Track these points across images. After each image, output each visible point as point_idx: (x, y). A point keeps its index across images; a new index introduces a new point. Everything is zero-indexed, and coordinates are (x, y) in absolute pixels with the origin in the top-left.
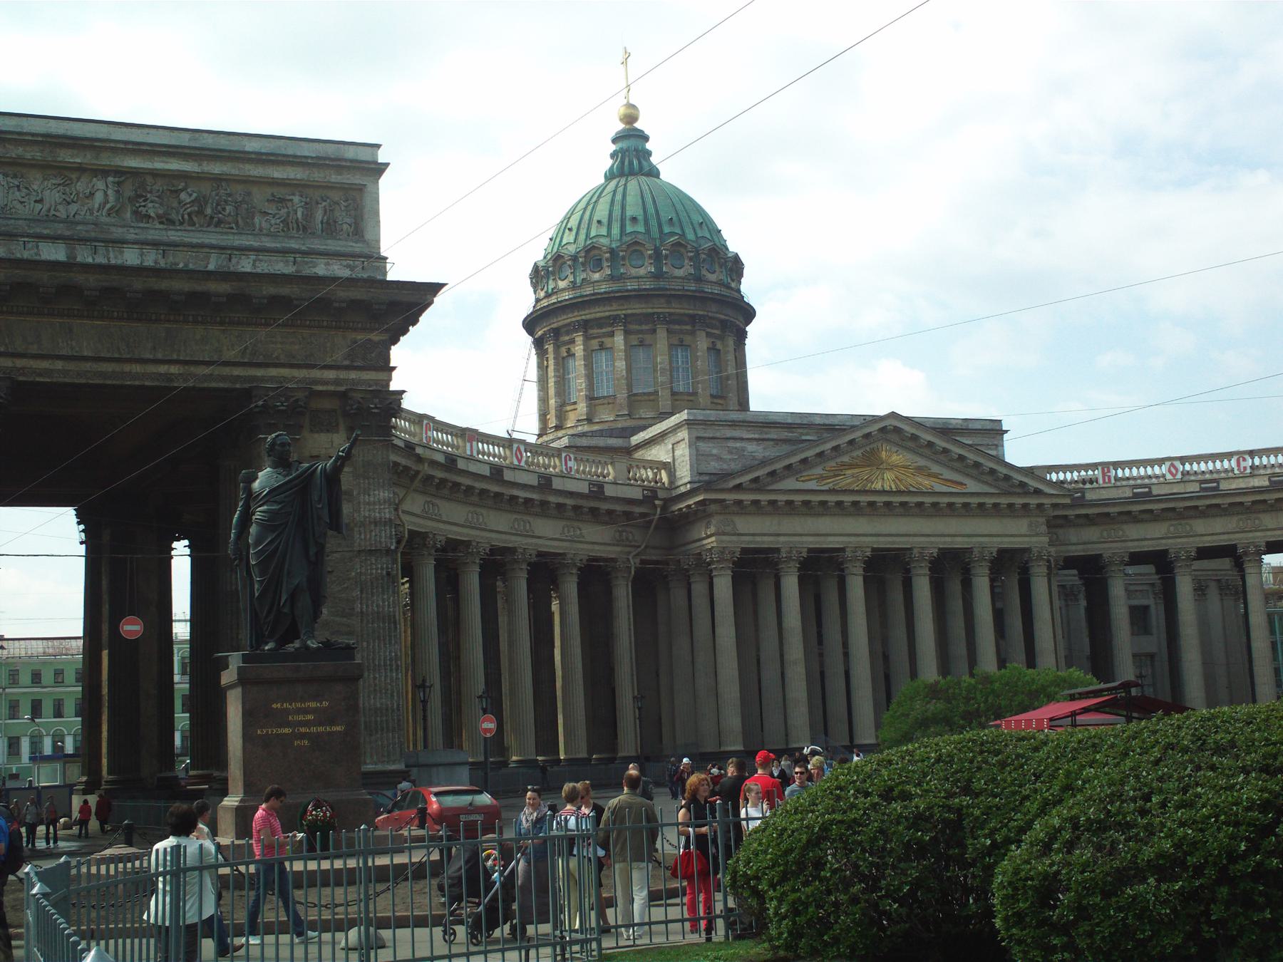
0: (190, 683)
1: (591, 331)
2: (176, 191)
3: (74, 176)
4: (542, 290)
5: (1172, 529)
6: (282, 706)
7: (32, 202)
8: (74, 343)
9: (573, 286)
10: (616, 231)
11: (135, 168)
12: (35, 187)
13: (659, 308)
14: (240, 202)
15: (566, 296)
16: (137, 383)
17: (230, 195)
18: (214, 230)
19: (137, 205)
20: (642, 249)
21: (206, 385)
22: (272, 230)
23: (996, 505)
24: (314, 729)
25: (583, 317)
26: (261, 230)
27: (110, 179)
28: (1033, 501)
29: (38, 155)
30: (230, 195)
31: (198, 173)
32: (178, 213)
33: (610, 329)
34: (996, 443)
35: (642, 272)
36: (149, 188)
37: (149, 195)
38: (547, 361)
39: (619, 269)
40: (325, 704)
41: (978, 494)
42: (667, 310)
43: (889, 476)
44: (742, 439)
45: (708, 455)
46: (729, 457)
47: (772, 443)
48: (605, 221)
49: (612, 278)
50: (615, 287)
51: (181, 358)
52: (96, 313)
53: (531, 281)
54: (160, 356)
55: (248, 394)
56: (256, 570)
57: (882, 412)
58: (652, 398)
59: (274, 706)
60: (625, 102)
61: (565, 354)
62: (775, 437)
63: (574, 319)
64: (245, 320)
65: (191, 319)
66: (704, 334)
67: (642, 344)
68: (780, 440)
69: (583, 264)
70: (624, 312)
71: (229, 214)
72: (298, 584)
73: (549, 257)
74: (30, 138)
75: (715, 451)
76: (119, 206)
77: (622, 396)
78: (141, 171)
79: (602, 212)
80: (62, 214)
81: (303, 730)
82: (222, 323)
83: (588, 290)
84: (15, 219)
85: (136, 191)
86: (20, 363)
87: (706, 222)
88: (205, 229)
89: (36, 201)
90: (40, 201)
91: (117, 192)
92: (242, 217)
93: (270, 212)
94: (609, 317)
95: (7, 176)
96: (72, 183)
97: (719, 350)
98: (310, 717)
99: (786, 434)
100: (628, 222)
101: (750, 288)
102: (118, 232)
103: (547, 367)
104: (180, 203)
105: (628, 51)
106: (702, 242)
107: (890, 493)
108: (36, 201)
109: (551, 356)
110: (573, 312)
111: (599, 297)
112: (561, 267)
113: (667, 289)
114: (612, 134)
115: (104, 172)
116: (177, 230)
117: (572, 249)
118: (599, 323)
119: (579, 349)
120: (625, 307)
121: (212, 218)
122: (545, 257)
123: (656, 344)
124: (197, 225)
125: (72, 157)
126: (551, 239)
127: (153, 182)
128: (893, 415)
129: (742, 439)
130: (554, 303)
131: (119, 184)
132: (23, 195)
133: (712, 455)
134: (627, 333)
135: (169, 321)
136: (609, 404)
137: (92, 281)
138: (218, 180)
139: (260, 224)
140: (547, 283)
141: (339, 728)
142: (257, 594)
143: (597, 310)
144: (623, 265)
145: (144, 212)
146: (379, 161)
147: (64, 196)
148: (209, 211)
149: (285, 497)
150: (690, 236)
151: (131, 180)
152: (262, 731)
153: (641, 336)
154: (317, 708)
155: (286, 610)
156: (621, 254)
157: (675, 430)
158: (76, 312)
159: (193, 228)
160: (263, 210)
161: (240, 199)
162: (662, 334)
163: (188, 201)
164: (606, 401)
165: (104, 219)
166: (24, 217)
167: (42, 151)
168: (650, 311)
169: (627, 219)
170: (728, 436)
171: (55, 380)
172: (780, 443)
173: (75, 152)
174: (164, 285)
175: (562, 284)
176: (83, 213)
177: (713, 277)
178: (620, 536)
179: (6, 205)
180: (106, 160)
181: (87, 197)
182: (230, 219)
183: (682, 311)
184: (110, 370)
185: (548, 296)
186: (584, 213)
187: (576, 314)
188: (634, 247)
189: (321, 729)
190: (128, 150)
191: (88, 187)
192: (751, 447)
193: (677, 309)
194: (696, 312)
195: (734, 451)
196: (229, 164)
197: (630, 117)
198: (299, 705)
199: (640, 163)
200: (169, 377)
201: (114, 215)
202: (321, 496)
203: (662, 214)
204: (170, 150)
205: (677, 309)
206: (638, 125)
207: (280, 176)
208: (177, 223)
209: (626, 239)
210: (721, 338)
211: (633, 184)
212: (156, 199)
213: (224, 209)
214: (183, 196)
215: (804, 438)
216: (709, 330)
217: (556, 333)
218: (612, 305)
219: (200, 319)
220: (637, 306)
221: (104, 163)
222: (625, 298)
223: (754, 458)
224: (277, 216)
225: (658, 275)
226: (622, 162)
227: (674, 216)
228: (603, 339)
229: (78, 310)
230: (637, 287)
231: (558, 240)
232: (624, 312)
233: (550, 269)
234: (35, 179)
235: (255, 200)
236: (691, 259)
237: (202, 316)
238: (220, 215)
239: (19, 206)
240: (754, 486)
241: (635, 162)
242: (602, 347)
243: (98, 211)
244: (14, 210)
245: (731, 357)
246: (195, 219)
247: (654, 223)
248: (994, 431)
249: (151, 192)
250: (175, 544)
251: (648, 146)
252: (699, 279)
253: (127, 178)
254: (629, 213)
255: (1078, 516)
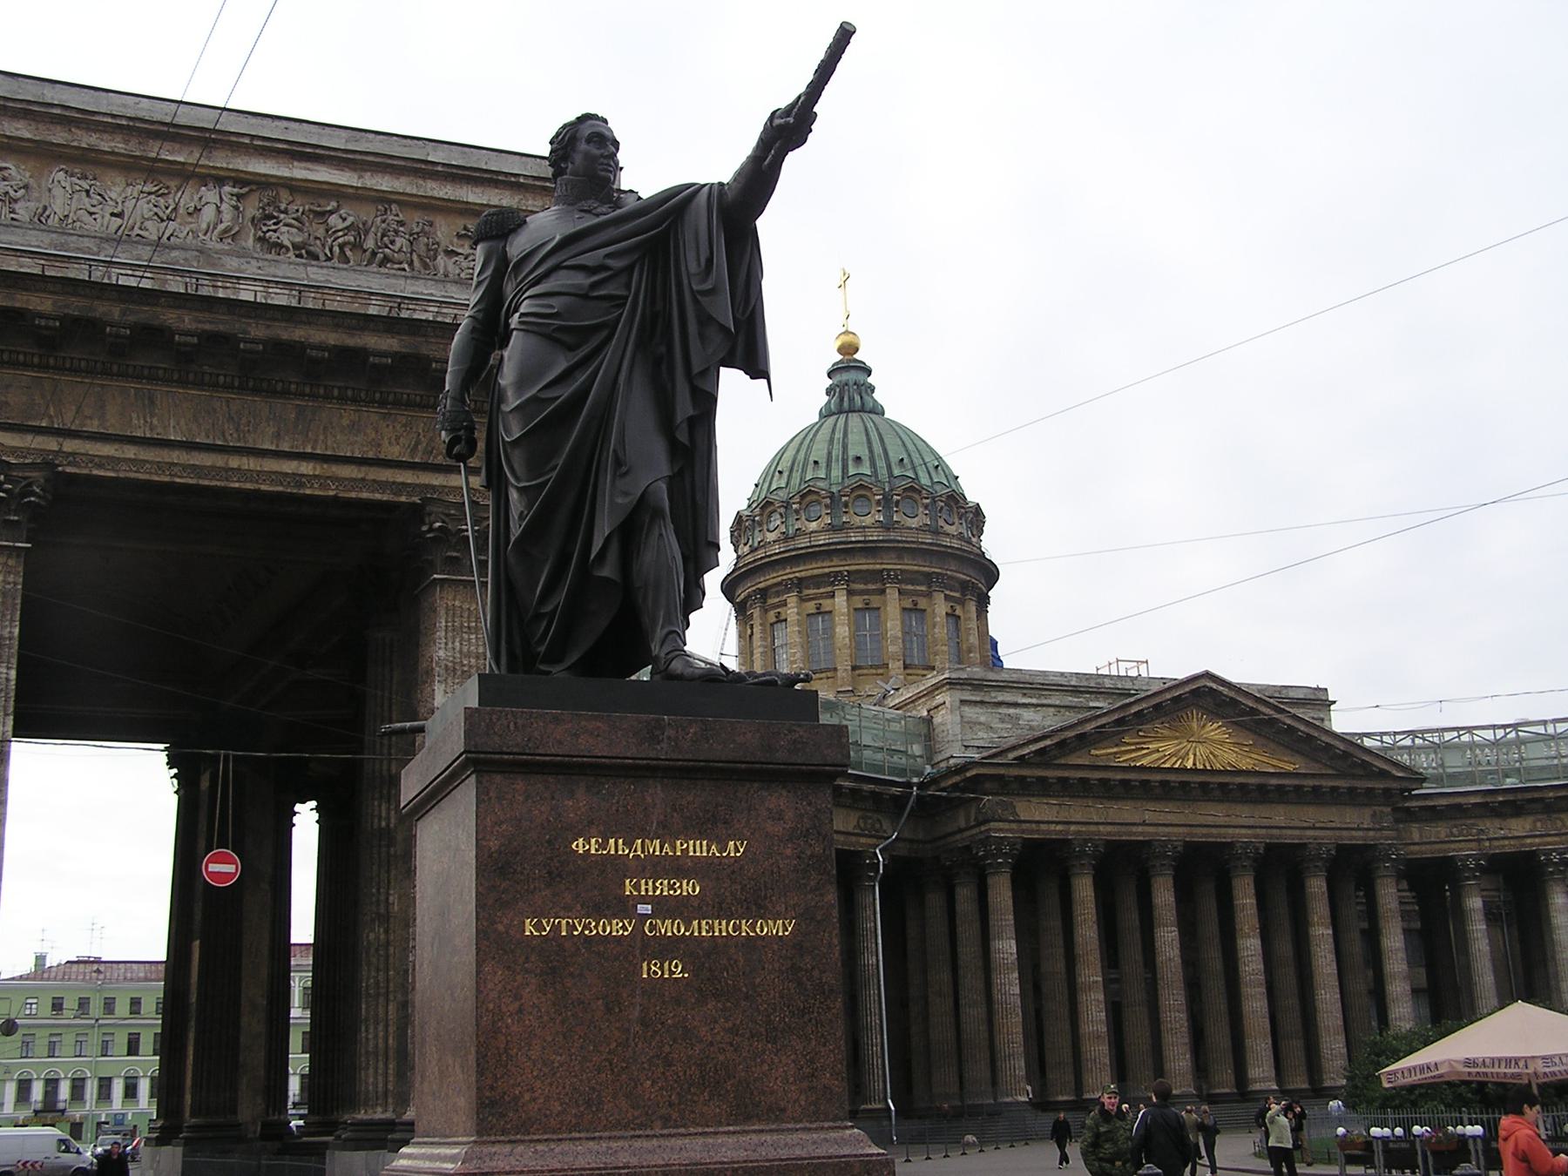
0: (313, 971)
1: (806, 592)
2: (323, 214)
3: (173, 184)
4: (745, 544)
5: (1539, 824)
6: (603, 846)
7: (108, 216)
8: (155, 421)
9: (786, 538)
10: (836, 472)
11: (265, 175)
12: (114, 196)
13: (889, 564)
14: (418, 233)
15: (776, 549)
16: (249, 486)
17: (401, 223)
18: (375, 270)
19: (265, 229)
20: (868, 494)
21: (353, 495)
22: (463, 275)
23: (1334, 789)
24: (701, 928)
25: (797, 575)
26: (446, 276)
27: (227, 189)
28: (1379, 785)
29: (120, 147)
30: (401, 223)
31: (357, 188)
32: (323, 245)
33: (829, 589)
34: (1322, 716)
35: (868, 520)
36: (283, 206)
37: (282, 216)
38: (752, 626)
39: (841, 517)
40: (735, 849)
41: (1313, 776)
42: (899, 567)
43: (1201, 749)
44: (1016, 705)
45: (975, 723)
46: (1000, 726)
47: (1052, 709)
48: (823, 464)
49: (832, 528)
50: (837, 537)
51: (319, 452)
52: (191, 376)
53: (732, 536)
54: (285, 447)
55: (416, 513)
56: (518, 457)
57: (1181, 673)
58: (880, 671)
59: (579, 845)
60: (844, 330)
61: (774, 620)
62: (1058, 703)
63: (785, 577)
64: (418, 398)
65: (336, 392)
66: (943, 595)
67: (867, 608)
68: (1063, 707)
69: (797, 512)
70: (847, 568)
71: (400, 250)
72: (643, 495)
73: (754, 506)
74: (110, 120)
75: (982, 719)
76: (237, 229)
77: (844, 666)
78: (272, 180)
79: (819, 452)
80: (153, 231)
81: (669, 928)
82: (383, 403)
83: (803, 542)
84: (80, 236)
85: (264, 209)
86: (70, 445)
87: (940, 465)
88: (364, 268)
89: (113, 214)
90: (120, 215)
91: (236, 208)
92: (419, 256)
93: (460, 251)
94: (828, 575)
95: (72, 176)
96: (169, 193)
97: (959, 617)
98: (689, 888)
99: (1070, 698)
100: (850, 463)
101: (992, 544)
102: (231, 265)
103: (751, 636)
104: (327, 231)
105: (847, 272)
106: (938, 487)
107: (1204, 771)
108: (113, 214)
109: (757, 622)
110: (785, 569)
111: (817, 549)
112: (770, 516)
113: (899, 542)
114: (828, 366)
115: (219, 179)
116: (322, 267)
117: (783, 495)
118: (817, 581)
119: (791, 612)
120: (849, 562)
121: (374, 254)
122: (749, 506)
123: (885, 603)
124: (352, 263)
125: (171, 153)
126: (757, 485)
127: (291, 198)
128: (1208, 675)
129: (1016, 705)
130: (762, 558)
131: (239, 197)
132: (95, 203)
133: (980, 723)
134: (850, 593)
135: (302, 395)
136: (828, 678)
137: (187, 321)
138: (383, 200)
139: (445, 267)
140: (753, 535)
141: (777, 928)
142: (516, 531)
143: (814, 565)
144: (846, 512)
145: (274, 239)
146: (622, 188)
147: (155, 209)
148: (370, 244)
149: (608, 256)
150: (925, 480)
151: (257, 194)
152: (539, 927)
153: (866, 597)
154: (709, 862)
155: (608, 571)
156: (844, 499)
157: (933, 691)
158: (161, 372)
159: (345, 266)
160: (451, 248)
161: (416, 230)
162: (892, 594)
163: (340, 227)
164: (823, 675)
165: (214, 244)
166: (93, 234)
167: (126, 142)
168: (878, 567)
169: (850, 458)
170: (1000, 699)
171: (122, 475)
172: (1062, 710)
173: (177, 146)
174: (298, 334)
175: (771, 537)
176: (181, 235)
177: (947, 528)
178: (865, 823)
179: (66, 216)
180: (221, 161)
181: (189, 214)
182: (401, 256)
183: (916, 568)
184: (209, 464)
185: (753, 550)
186: (798, 451)
187: (788, 571)
188: (860, 490)
189: (723, 928)
190: (256, 148)
191: (192, 200)
192: (1028, 715)
193: (910, 565)
194: (933, 570)
195: (1007, 719)
196: (403, 179)
197: (849, 349)
198: (655, 847)
199: (861, 398)
200: (298, 479)
201: (230, 241)
202: (710, 261)
203: (891, 454)
204: (317, 151)
205: (910, 565)
206: (856, 356)
207: (479, 201)
208: (322, 257)
209: (847, 482)
210: (962, 602)
211: (854, 419)
212: (293, 222)
213: (392, 242)
214: (333, 220)
215: (1092, 704)
216: (947, 592)
217: (764, 593)
218: (832, 561)
219: (350, 393)
220: (864, 561)
221: (219, 165)
222: (849, 551)
223: (1031, 728)
224: (470, 258)
225: (888, 526)
226: (842, 399)
227: (905, 456)
228: (821, 601)
229: (165, 369)
230: (862, 539)
231: (766, 485)
232: (847, 568)
233: (757, 518)
234: (114, 184)
235: (439, 233)
236: (926, 507)
237: (353, 389)
238: (387, 250)
239: (90, 219)
240: (1038, 759)
241: (857, 398)
242: (819, 612)
243: (205, 234)
244: (78, 224)
245: (973, 624)
246: (349, 253)
247: (881, 464)
248: (1319, 700)
249: (285, 212)
250: (298, 807)
251: (870, 380)
252: (936, 532)
253: (251, 190)
254: (852, 453)
255: (1421, 808)
